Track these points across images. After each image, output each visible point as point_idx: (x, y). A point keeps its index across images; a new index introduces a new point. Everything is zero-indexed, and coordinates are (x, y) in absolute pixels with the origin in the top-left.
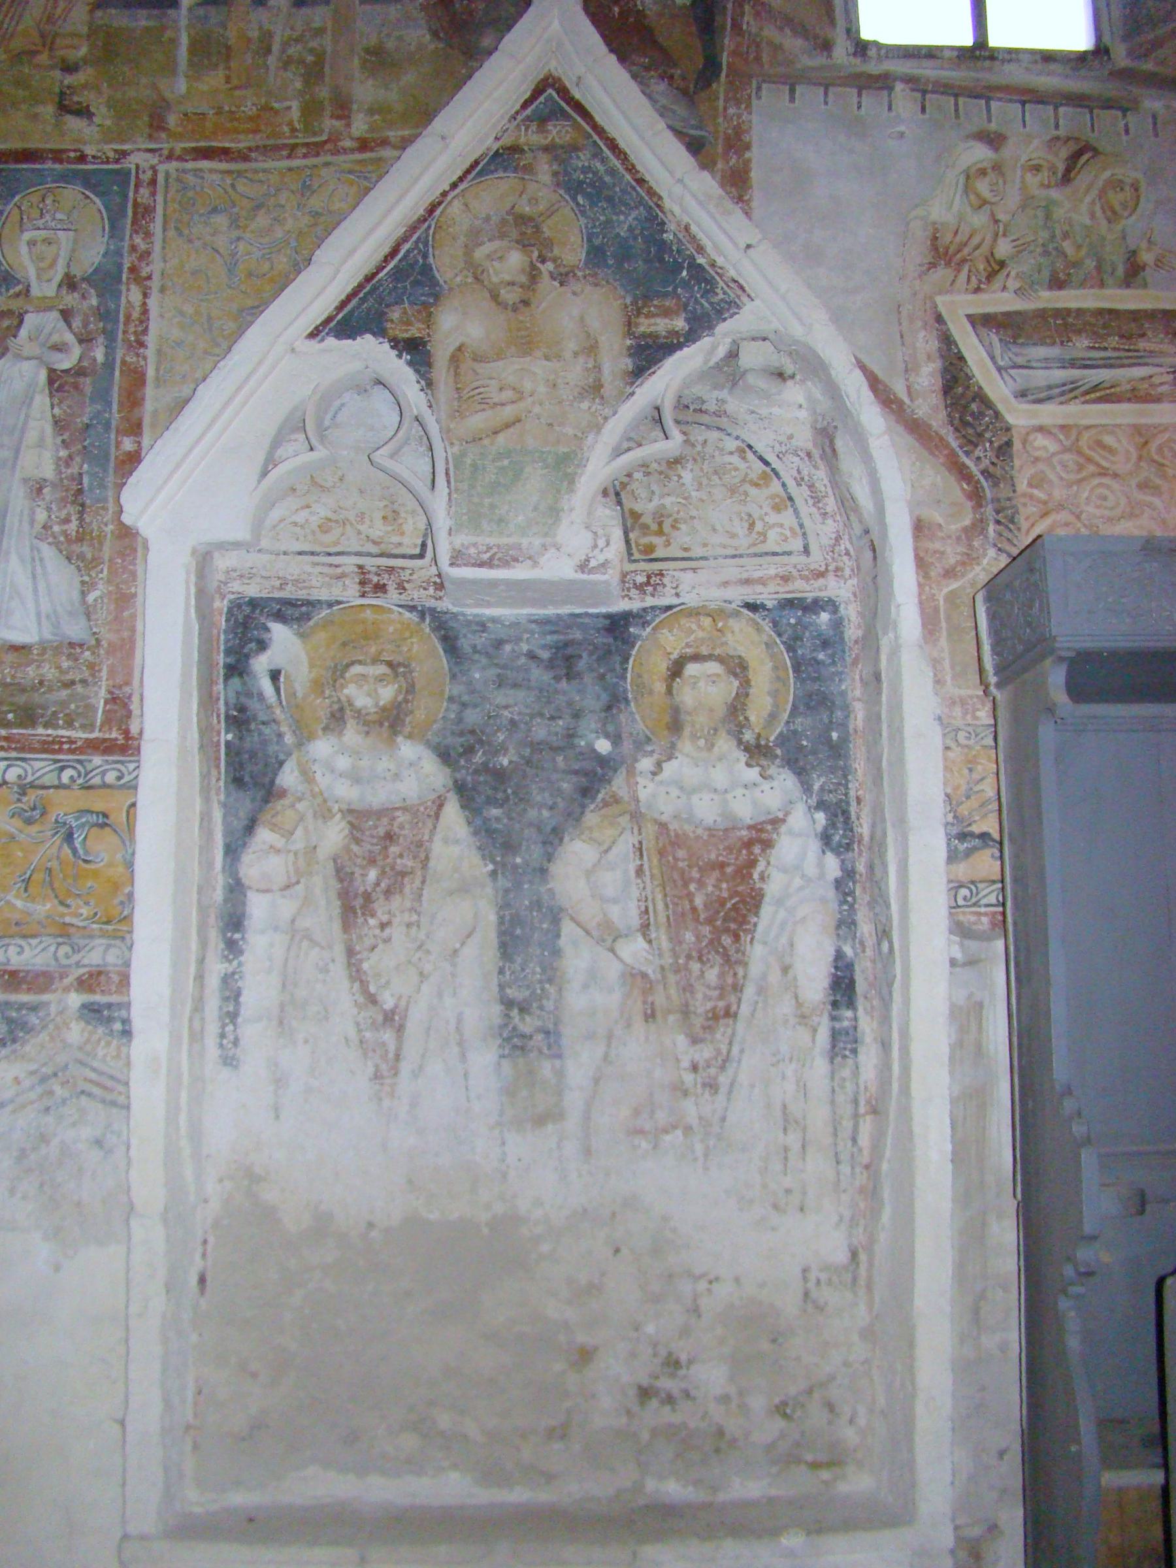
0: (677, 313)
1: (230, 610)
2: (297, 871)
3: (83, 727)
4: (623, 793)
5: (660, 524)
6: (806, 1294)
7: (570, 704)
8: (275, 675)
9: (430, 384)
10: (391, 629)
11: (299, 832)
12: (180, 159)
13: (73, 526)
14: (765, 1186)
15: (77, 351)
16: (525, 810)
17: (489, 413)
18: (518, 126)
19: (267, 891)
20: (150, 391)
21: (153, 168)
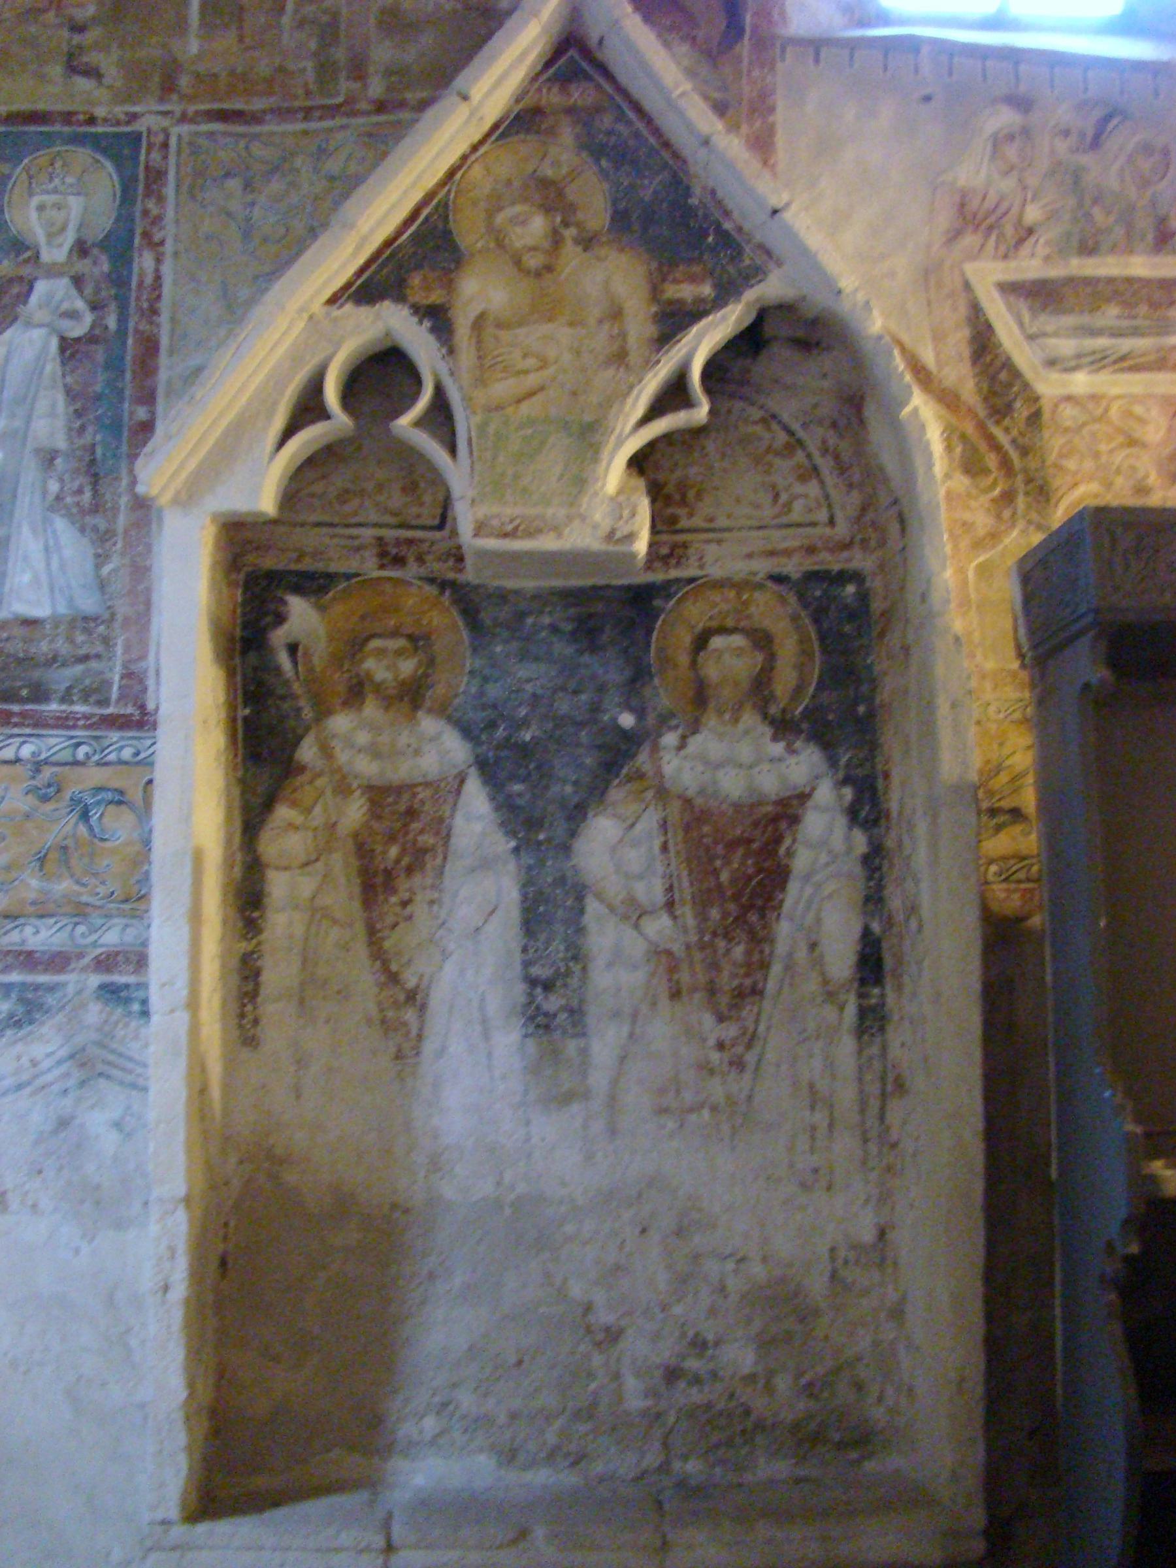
0: (703, 281)
4: (647, 768)
5: (684, 496)
6: (834, 1275)
7: (594, 677)
8: (293, 649)
9: (451, 351)
10: (411, 602)
11: (318, 810)
12: (192, 121)
13: (87, 495)
14: (791, 1165)
15: (89, 318)
16: (547, 788)
17: (511, 381)
18: (539, 90)
19: (286, 868)
20: (163, 360)
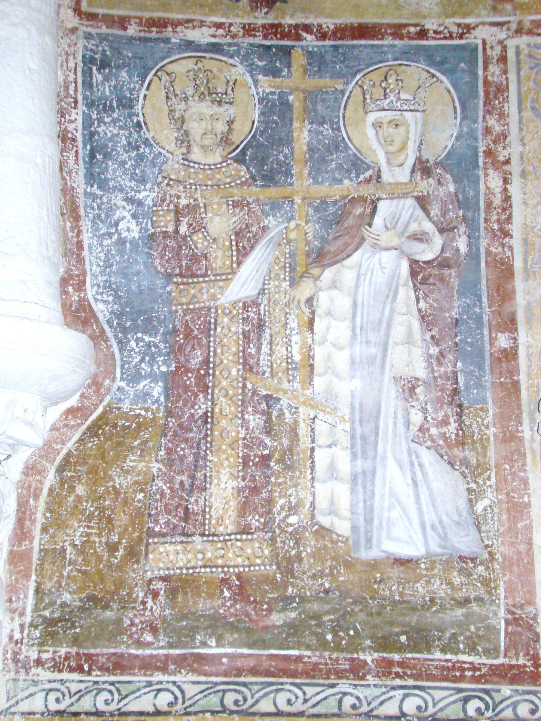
3: (487, 652)
12: (530, 32)
13: (453, 427)
15: (438, 241)
20: (519, 284)
21: (500, 42)
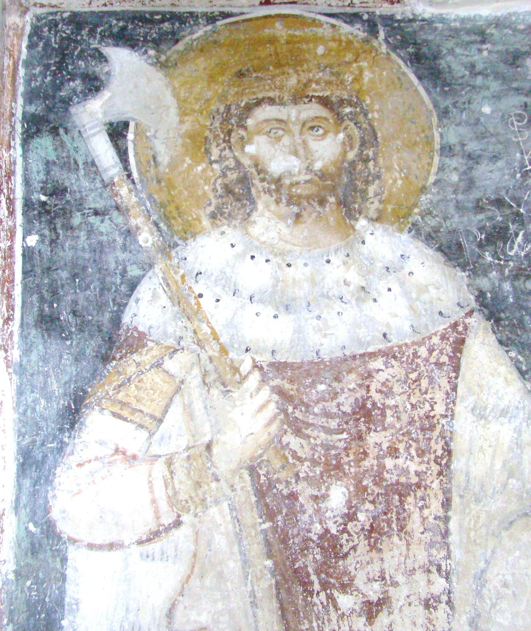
1: (36, 31)
2: (173, 500)
8: (117, 132)
10: (320, 50)
11: (176, 413)
19: (111, 546)
